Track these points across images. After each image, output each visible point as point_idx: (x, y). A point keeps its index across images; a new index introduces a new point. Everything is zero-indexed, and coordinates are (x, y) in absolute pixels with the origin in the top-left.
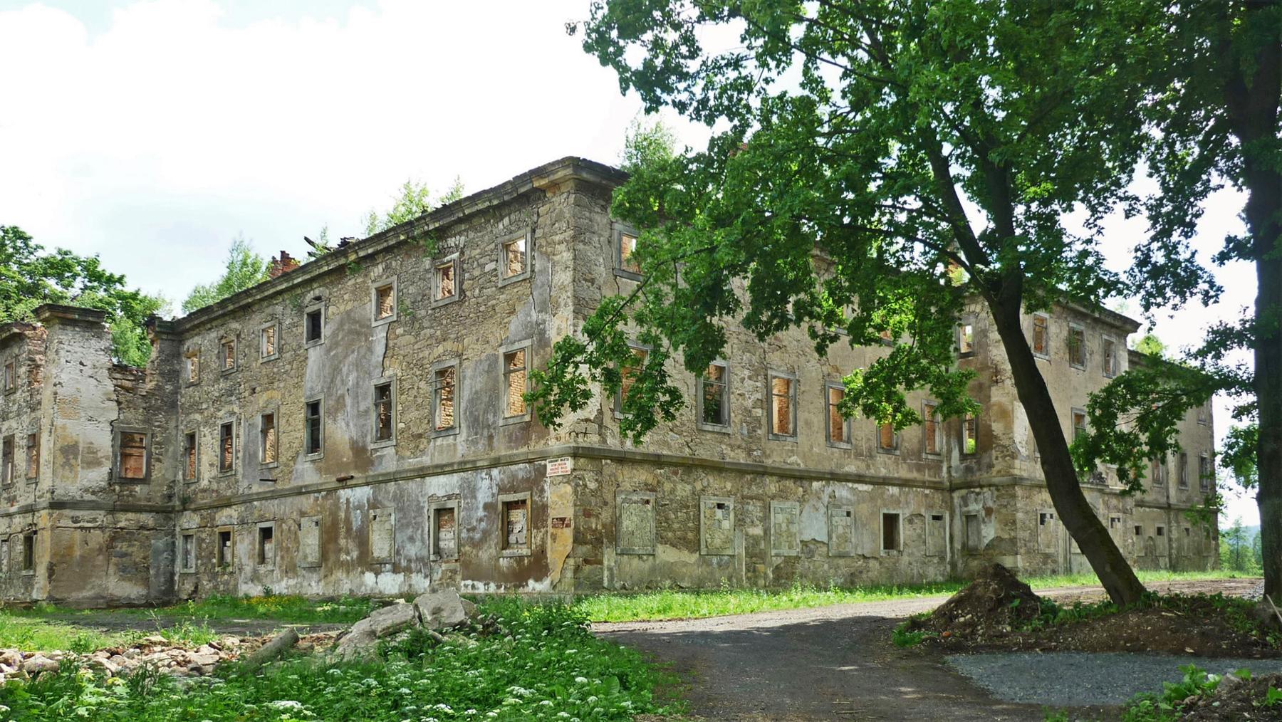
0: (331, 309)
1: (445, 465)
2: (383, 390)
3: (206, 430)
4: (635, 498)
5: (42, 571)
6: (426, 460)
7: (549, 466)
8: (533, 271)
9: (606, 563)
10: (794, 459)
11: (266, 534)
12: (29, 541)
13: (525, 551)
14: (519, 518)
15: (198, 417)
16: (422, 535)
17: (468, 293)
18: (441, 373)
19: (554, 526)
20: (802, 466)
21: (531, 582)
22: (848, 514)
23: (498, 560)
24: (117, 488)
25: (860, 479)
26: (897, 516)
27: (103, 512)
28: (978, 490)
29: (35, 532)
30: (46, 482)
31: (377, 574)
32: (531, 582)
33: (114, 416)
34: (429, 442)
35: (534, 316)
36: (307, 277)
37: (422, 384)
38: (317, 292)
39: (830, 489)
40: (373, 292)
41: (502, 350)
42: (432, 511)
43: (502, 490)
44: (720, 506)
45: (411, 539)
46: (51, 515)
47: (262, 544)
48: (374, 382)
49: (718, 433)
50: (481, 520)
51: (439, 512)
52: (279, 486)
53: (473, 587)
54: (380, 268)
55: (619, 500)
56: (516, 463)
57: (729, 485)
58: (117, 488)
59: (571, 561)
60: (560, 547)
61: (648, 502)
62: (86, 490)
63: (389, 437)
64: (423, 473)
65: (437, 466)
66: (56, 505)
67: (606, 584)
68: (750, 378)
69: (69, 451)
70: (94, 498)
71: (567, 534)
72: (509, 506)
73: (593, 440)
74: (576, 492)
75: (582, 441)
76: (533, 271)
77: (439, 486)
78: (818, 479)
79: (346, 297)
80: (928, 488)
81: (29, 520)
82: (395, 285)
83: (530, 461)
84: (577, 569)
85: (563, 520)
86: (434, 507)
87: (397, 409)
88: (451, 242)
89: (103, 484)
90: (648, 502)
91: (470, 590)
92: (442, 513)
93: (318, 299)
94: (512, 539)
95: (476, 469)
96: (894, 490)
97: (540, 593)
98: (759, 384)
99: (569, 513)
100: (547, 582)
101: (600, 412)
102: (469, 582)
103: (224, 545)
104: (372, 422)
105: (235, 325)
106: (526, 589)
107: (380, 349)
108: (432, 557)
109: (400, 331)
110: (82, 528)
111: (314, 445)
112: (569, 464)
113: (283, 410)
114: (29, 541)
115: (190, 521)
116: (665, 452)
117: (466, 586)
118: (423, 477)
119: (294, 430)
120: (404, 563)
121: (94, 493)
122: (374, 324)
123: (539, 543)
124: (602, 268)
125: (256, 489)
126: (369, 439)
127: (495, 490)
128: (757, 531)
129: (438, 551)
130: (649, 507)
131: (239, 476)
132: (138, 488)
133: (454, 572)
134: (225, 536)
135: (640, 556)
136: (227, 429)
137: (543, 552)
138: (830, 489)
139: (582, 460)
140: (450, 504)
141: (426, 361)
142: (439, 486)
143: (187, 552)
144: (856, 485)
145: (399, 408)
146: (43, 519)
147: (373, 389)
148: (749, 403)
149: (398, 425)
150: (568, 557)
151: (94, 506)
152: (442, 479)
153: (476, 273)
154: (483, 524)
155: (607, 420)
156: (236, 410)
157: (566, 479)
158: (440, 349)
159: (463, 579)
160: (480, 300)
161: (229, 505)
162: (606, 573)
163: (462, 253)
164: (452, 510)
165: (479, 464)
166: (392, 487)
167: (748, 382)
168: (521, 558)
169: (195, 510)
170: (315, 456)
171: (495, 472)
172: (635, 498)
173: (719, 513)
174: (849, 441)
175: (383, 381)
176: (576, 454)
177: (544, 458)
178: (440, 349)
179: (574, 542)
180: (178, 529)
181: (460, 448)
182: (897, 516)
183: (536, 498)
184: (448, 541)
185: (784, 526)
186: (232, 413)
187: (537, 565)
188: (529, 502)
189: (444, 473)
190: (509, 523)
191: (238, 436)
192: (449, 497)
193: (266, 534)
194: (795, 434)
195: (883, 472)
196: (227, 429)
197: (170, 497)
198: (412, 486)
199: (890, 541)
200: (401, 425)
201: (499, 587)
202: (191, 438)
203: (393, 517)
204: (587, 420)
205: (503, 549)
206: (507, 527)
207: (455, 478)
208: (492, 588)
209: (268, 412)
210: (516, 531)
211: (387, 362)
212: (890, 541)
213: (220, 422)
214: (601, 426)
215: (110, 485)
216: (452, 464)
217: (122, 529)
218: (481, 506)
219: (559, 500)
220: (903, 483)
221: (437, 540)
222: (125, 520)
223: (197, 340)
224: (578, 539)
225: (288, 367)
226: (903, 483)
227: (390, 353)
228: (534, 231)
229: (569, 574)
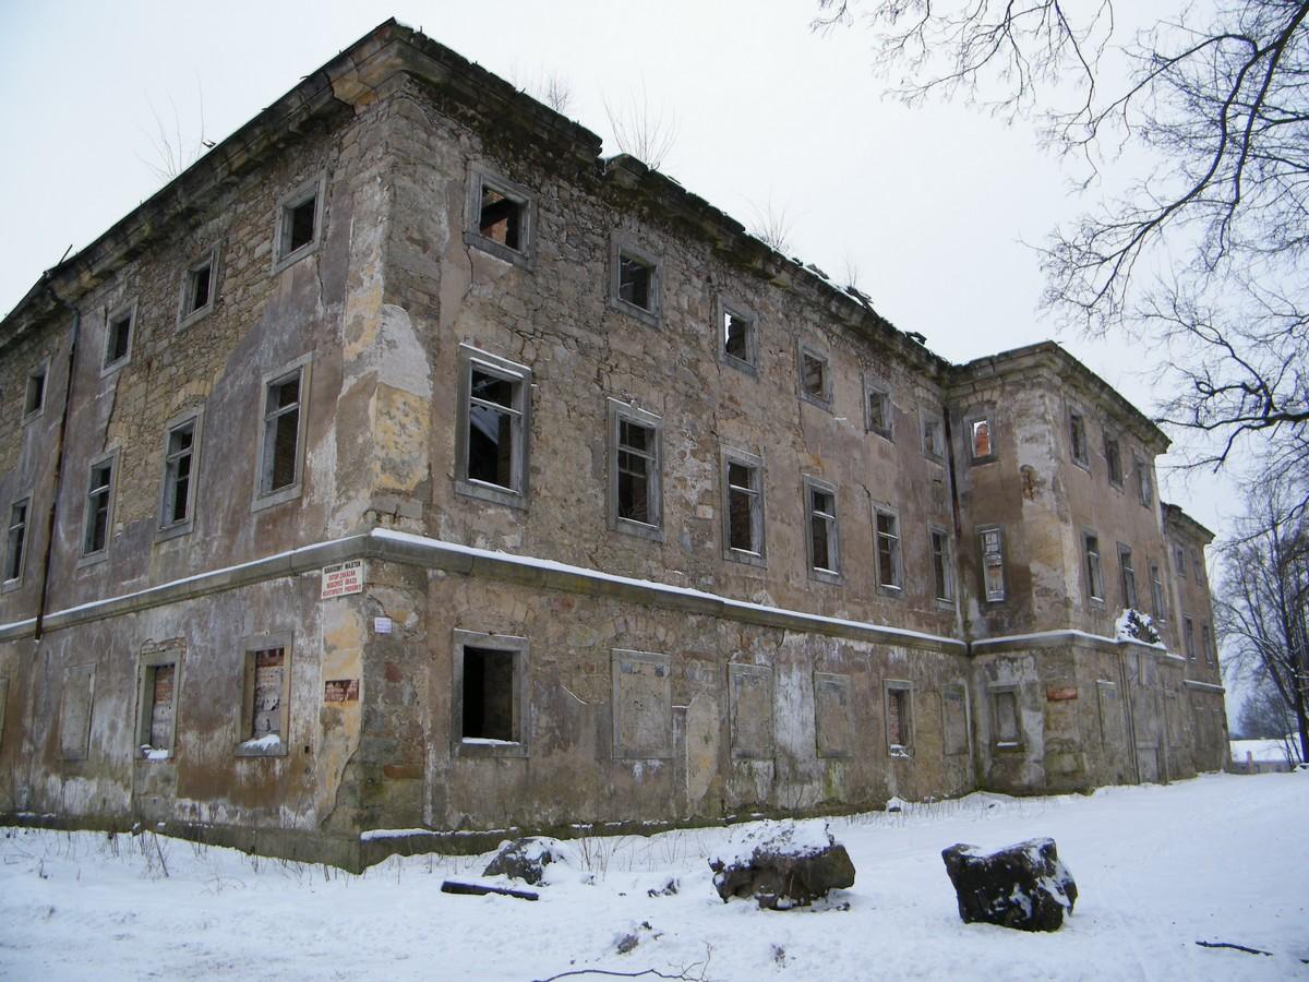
7: (326, 579)
16: (129, 710)
23: (232, 764)
42: (144, 669)
48: (94, 461)
53: (193, 809)
64: (138, 607)
77: (160, 624)
83: (294, 572)
85: (344, 684)
87: (117, 500)
102: (188, 802)
117: (183, 808)
123: (301, 731)
140: (169, 658)
141: (160, 419)
145: (120, 498)
148: (693, 496)
149: (115, 528)
155: (441, 493)
158: (180, 397)
159: (180, 795)
160: (242, 305)
175: (104, 458)
192: (170, 643)
198: (120, 625)
201: (232, 814)
210: (268, 707)
214: (429, 505)
227: (117, 413)
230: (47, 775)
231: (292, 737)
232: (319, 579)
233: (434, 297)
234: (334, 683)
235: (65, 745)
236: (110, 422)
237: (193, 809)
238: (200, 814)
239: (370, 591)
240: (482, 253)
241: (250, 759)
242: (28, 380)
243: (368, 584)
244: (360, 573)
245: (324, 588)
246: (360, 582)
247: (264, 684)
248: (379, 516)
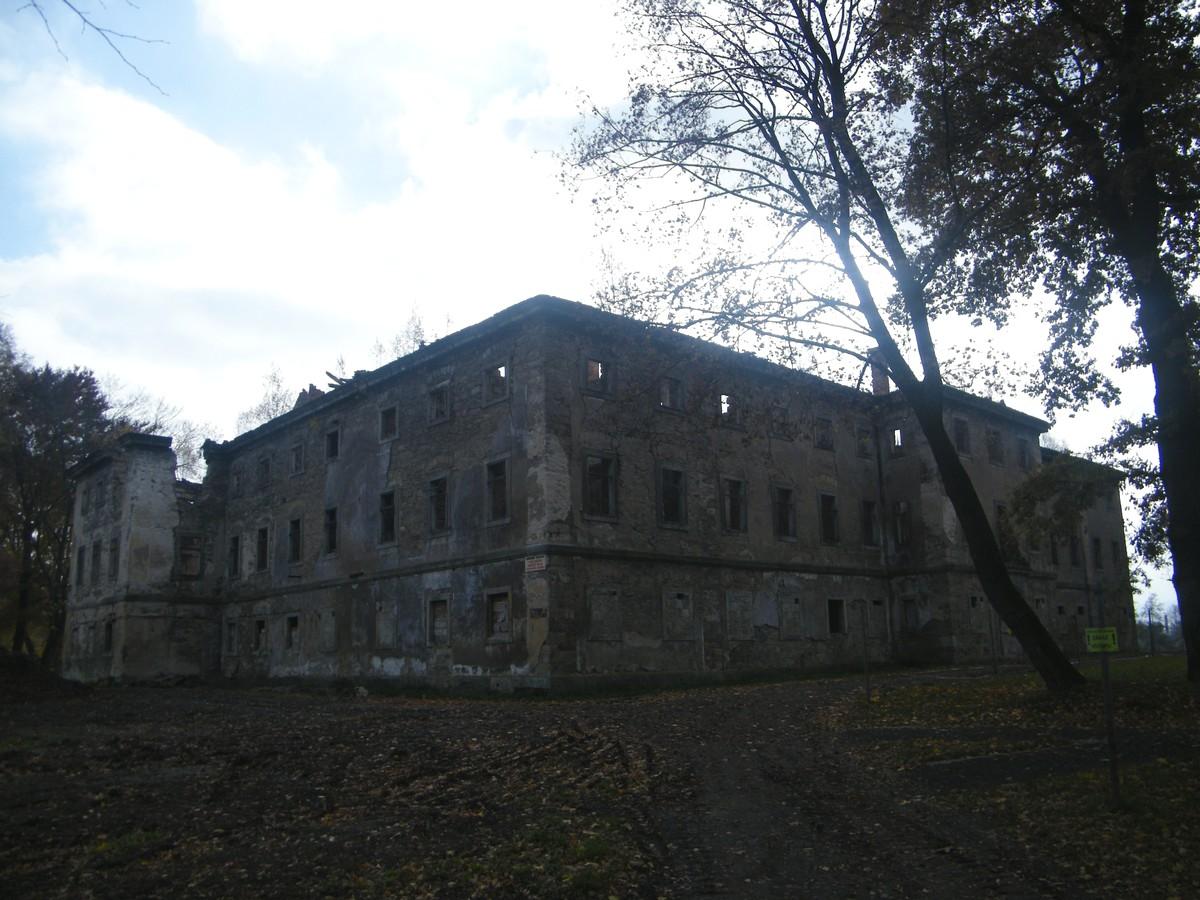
0: (347, 431)
1: (439, 563)
2: (388, 499)
3: (246, 535)
4: (604, 590)
5: (117, 653)
6: (423, 558)
7: (527, 563)
8: (511, 393)
9: (578, 648)
10: (746, 552)
11: (293, 623)
12: (109, 627)
13: (506, 638)
14: (502, 609)
15: (240, 523)
17: (458, 414)
18: (435, 483)
19: (532, 617)
20: (753, 559)
21: (513, 667)
22: (797, 601)
24: (177, 583)
25: (806, 569)
26: (841, 602)
27: (165, 604)
28: (913, 577)
29: (114, 621)
30: (123, 576)
31: (383, 659)
32: (513, 667)
33: (176, 523)
34: (425, 543)
35: (513, 430)
36: (326, 404)
37: (420, 493)
38: (335, 417)
39: (780, 578)
40: (380, 415)
41: (486, 462)
42: (428, 603)
43: (486, 583)
44: (680, 596)
45: (411, 628)
46: (125, 606)
47: (290, 631)
49: (676, 530)
50: (469, 611)
51: (435, 604)
52: (304, 581)
53: (463, 669)
54: (386, 394)
55: (589, 592)
56: (499, 560)
57: (688, 578)
58: (177, 583)
59: (547, 648)
60: (537, 632)
61: (615, 593)
62: (153, 585)
63: (392, 539)
64: (421, 570)
65: (431, 564)
66: (131, 598)
67: (579, 668)
68: (704, 481)
69: (141, 553)
70: (158, 592)
71: (542, 624)
72: (494, 598)
73: (565, 540)
74: (550, 584)
75: (555, 541)
76: (511, 393)
77: (433, 581)
78: (768, 570)
79: (358, 420)
80: (869, 576)
81: (110, 610)
82: (397, 409)
83: (510, 558)
84: (552, 656)
85: (540, 610)
86: (430, 599)
87: (399, 514)
88: (444, 371)
89: (166, 580)
90: (615, 593)
91: (461, 674)
92: (437, 604)
93: (336, 422)
94: (496, 627)
95: (465, 565)
96: (837, 579)
97: (520, 676)
98: (712, 486)
99: (545, 604)
100: (527, 666)
101: (571, 514)
102: (460, 666)
103: (260, 632)
104: (379, 526)
105: (271, 447)
106: (508, 673)
107: (385, 464)
108: (428, 644)
109: (401, 447)
110: (149, 617)
111: (332, 545)
112: (544, 561)
113: (307, 516)
114: (109, 627)
115: (234, 611)
116: (630, 549)
117: (457, 669)
118: (421, 573)
119: (314, 535)
120: (404, 649)
121: (159, 588)
122: (380, 442)
124: (571, 389)
125: (285, 584)
126: (376, 540)
127: (480, 584)
128: (714, 618)
129: (433, 638)
130: (616, 598)
131: (272, 574)
132: (193, 584)
133: (447, 656)
134: (261, 625)
135: (608, 643)
136: (263, 533)
137: (523, 639)
138: (780, 578)
139: (556, 557)
140: (445, 596)
142: (433, 581)
143: (231, 639)
144: (803, 575)
145: (401, 513)
146: (120, 609)
147: (379, 498)
150: (544, 643)
151: (158, 598)
152: (436, 575)
153: (464, 396)
154: (471, 615)
156: (271, 517)
157: (541, 573)
158: (435, 462)
159: (456, 663)
161: (264, 598)
162: (579, 658)
163: (452, 380)
164: (444, 602)
165: (468, 561)
166: (395, 582)
167: (702, 485)
168: (504, 643)
169: (237, 603)
170: (332, 556)
171: (481, 568)
172: (604, 590)
173: (680, 603)
174: (794, 535)
175: (388, 491)
176: (549, 551)
177: (522, 556)
178: (435, 462)
179: (550, 630)
180: (224, 618)
181: (451, 547)
182: (841, 602)
183: (517, 591)
184: (442, 629)
185: (739, 612)
186: (267, 520)
187: (517, 652)
188: (510, 595)
189: (437, 570)
190: (493, 613)
191: (271, 539)
192: (443, 590)
193: (293, 623)
194: (746, 530)
195: (827, 562)
196: (263, 533)
197: (218, 591)
199: (836, 623)
200: (403, 528)
201: (485, 671)
202: (236, 541)
203: (396, 608)
204: (559, 521)
205: (489, 636)
206: (492, 617)
207: (448, 573)
208: (480, 672)
209: (296, 518)
210: (500, 620)
211: (391, 475)
212: (836, 623)
213: (257, 528)
215: (172, 580)
216: (444, 562)
217: (180, 618)
218: (469, 598)
219: (537, 592)
220: (844, 572)
221: (433, 628)
222: (183, 610)
223: (241, 459)
224: (553, 627)
225: (311, 480)
226: (844, 572)
228: (512, 358)
229: (546, 660)
230: (371, 657)
231: (514, 634)
232: (523, 563)
233: (568, 426)
234: (535, 610)
235: (381, 641)
236: (388, 470)
237: (463, 669)
238: (468, 672)
239: (549, 569)
240: (590, 398)
241: (493, 645)
242: (326, 437)
243: (547, 566)
244: (544, 561)
245: (526, 567)
246: (544, 565)
247: (496, 610)
248: (551, 534)
